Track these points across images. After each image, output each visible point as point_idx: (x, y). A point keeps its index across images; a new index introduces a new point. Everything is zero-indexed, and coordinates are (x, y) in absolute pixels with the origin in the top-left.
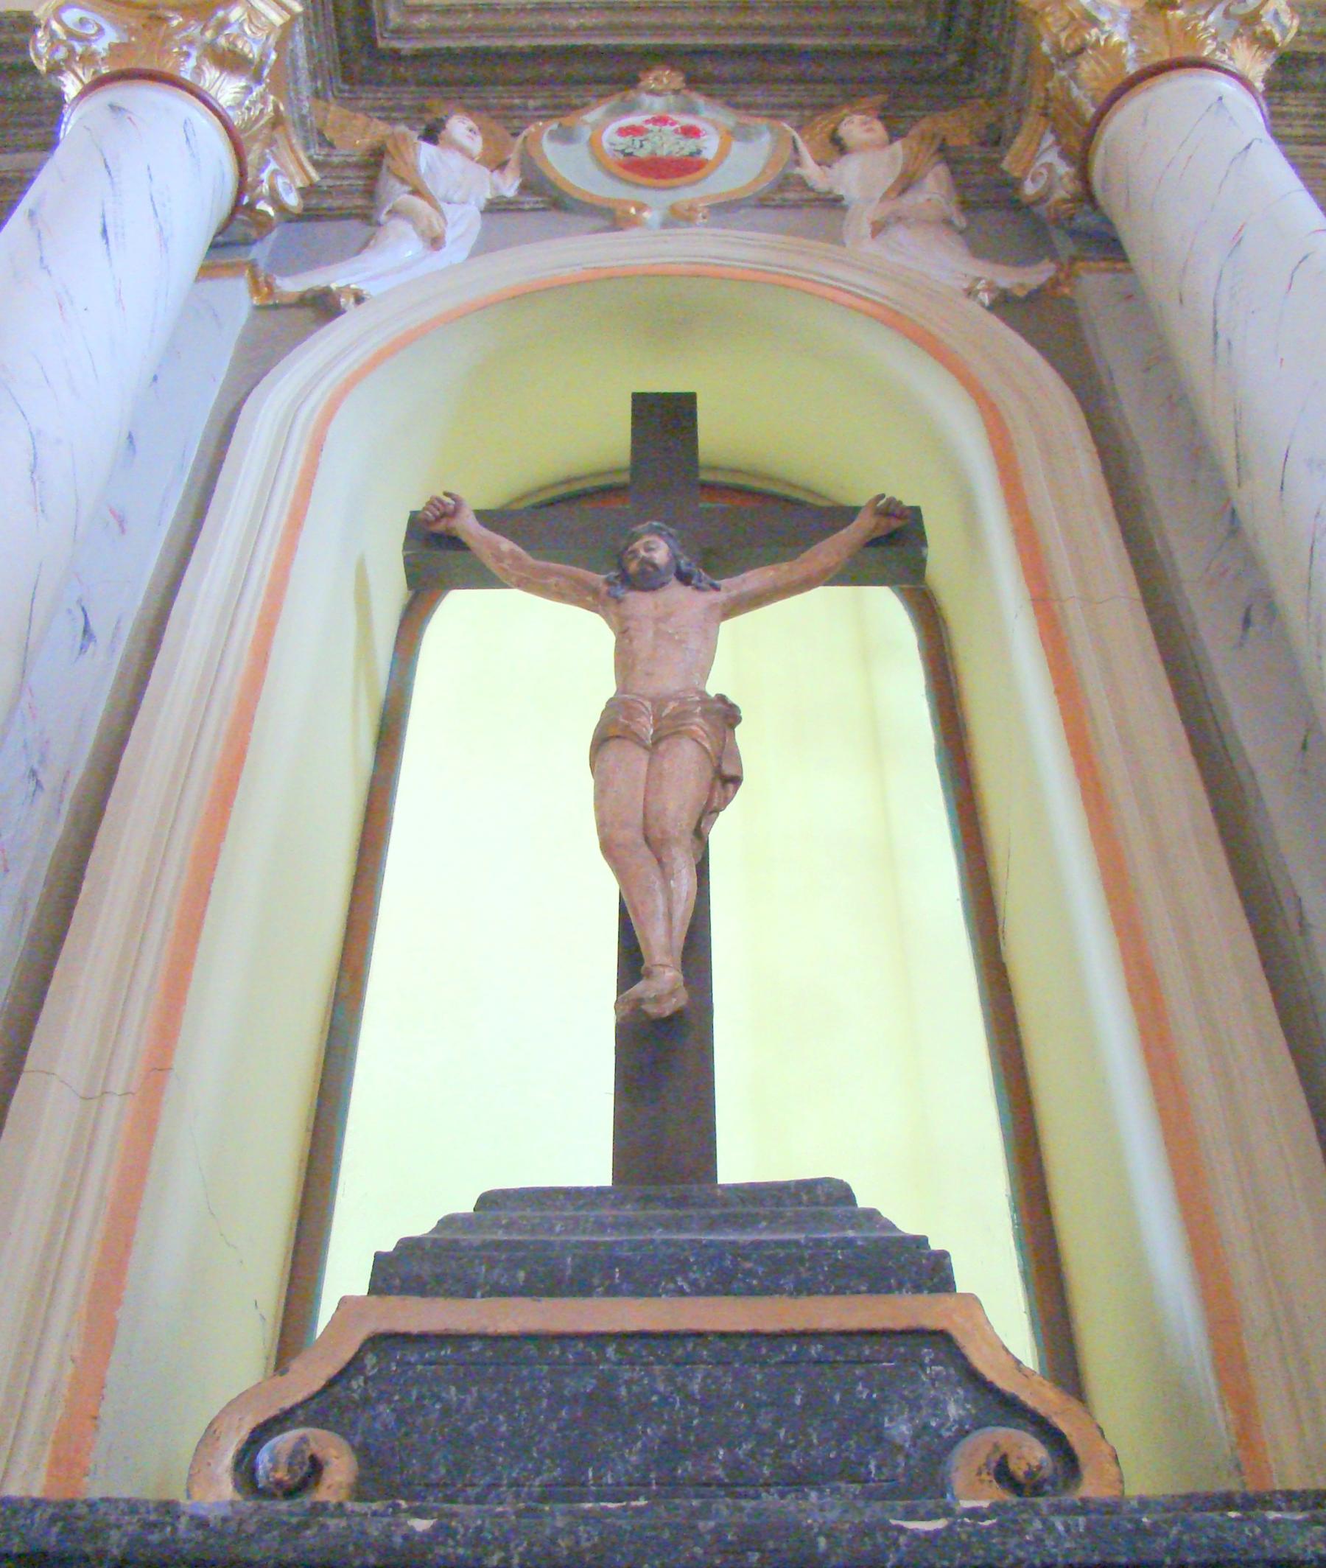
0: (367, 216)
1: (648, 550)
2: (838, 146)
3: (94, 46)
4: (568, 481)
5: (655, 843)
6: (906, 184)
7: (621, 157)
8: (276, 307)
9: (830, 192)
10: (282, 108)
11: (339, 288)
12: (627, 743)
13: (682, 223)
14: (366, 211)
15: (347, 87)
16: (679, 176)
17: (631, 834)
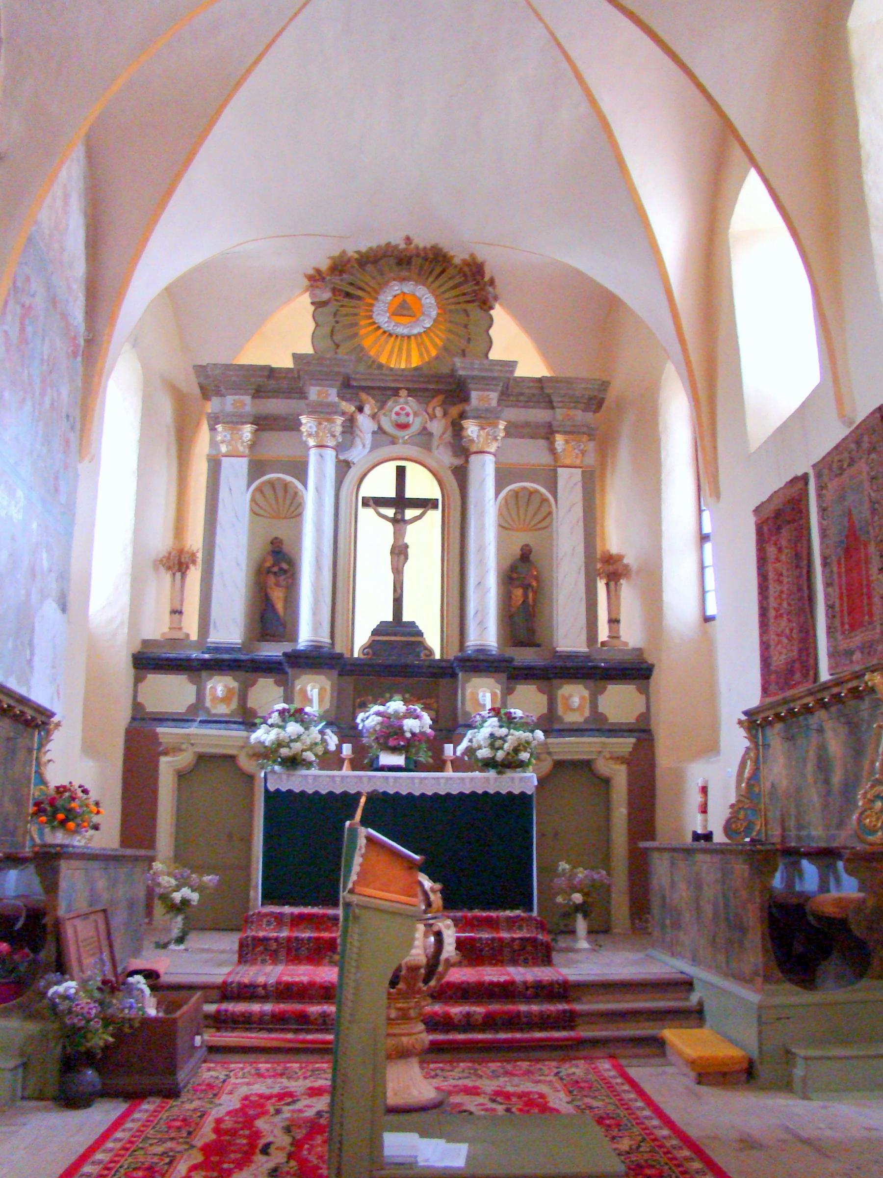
6: (444, 433)
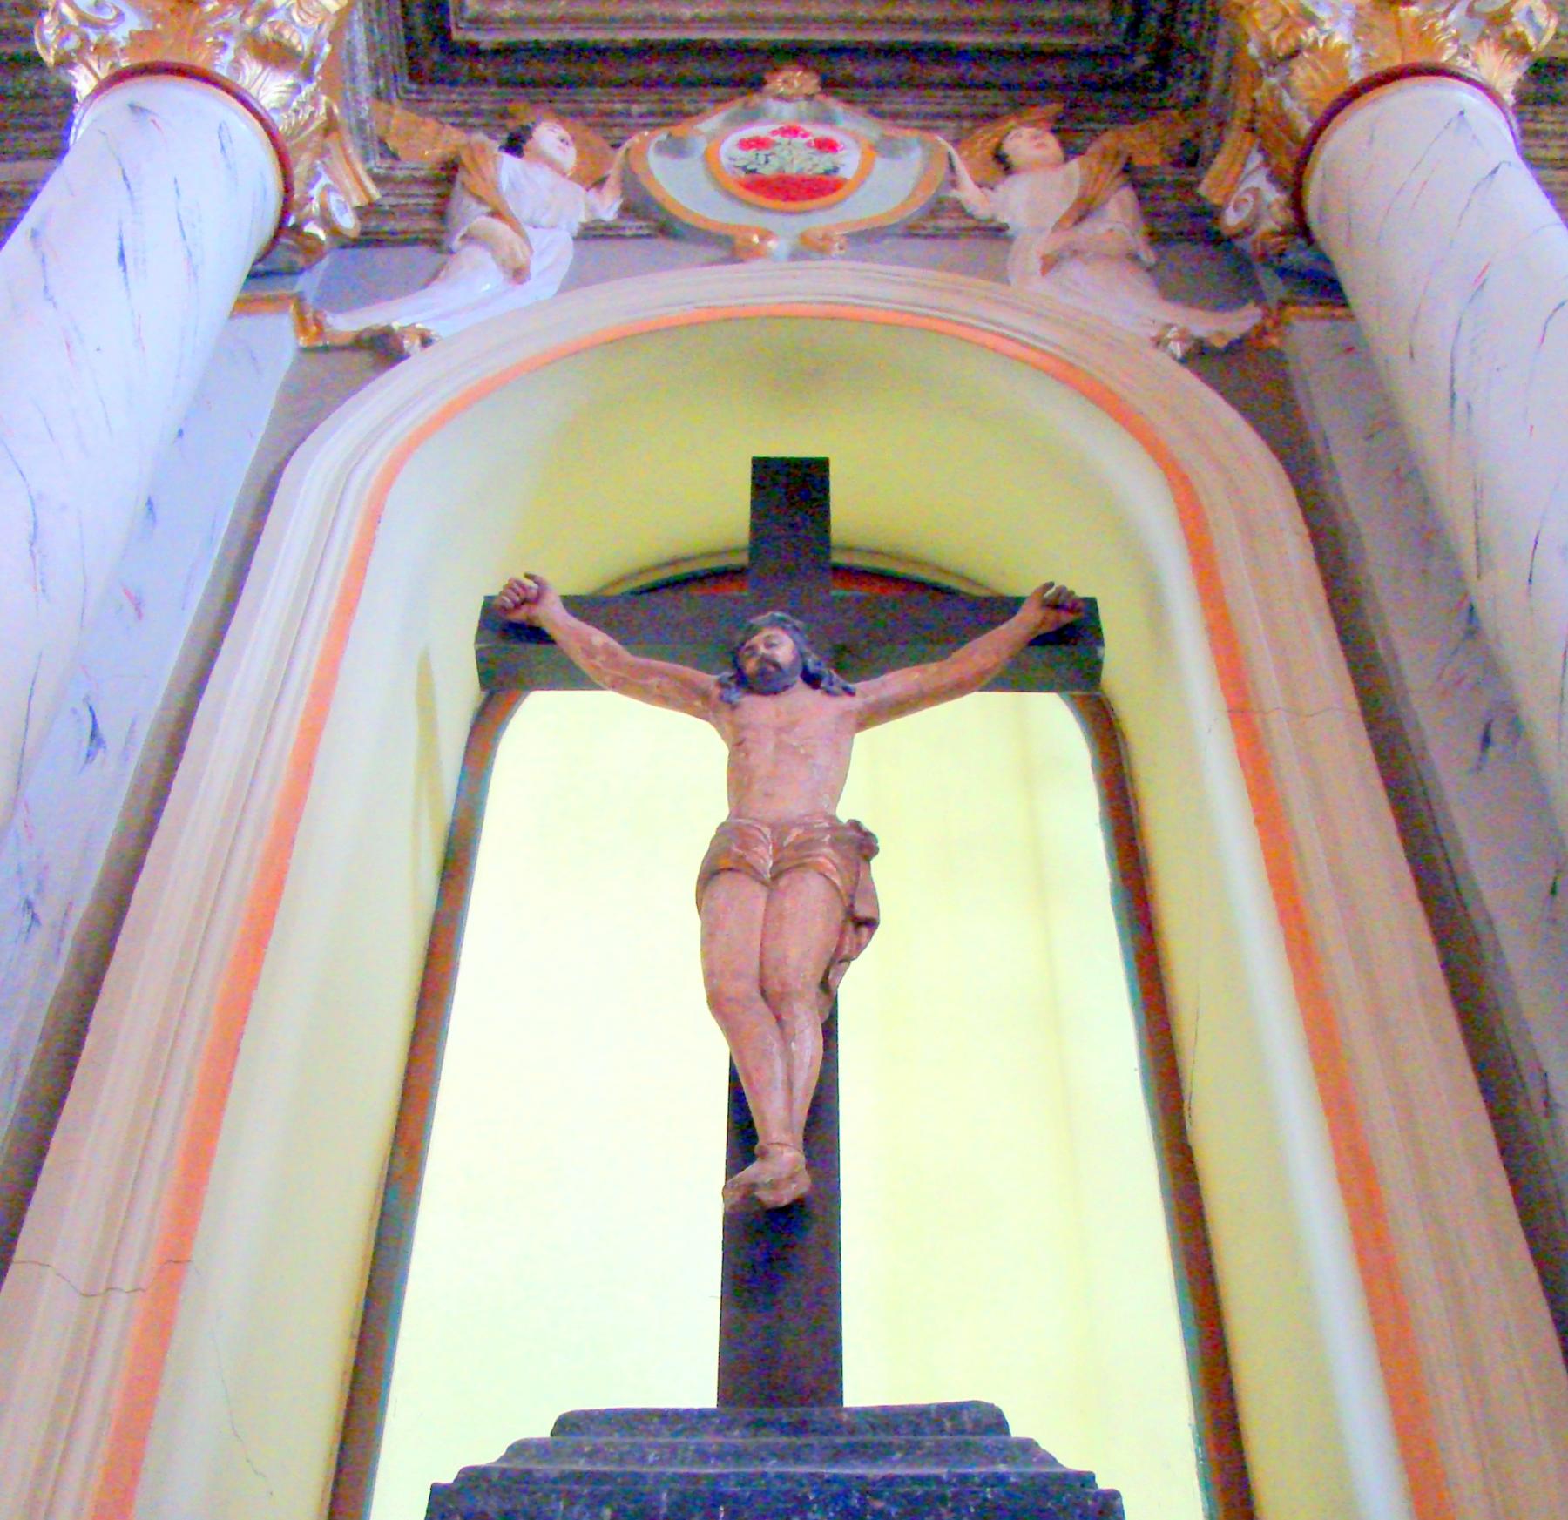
0: (435, 243)
1: (769, 646)
2: (1003, 163)
3: (112, 35)
4: (674, 562)
5: (773, 998)
6: (1083, 211)
7: (743, 174)
8: (326, 349)
9: (992, 220)
10: (336, 110)
11: (402, 328)
12: (741, 877)
13: (815, 255)
14: (436, 236)
15: (414, 87)
16: (812, 198)
17: (746, 987)
